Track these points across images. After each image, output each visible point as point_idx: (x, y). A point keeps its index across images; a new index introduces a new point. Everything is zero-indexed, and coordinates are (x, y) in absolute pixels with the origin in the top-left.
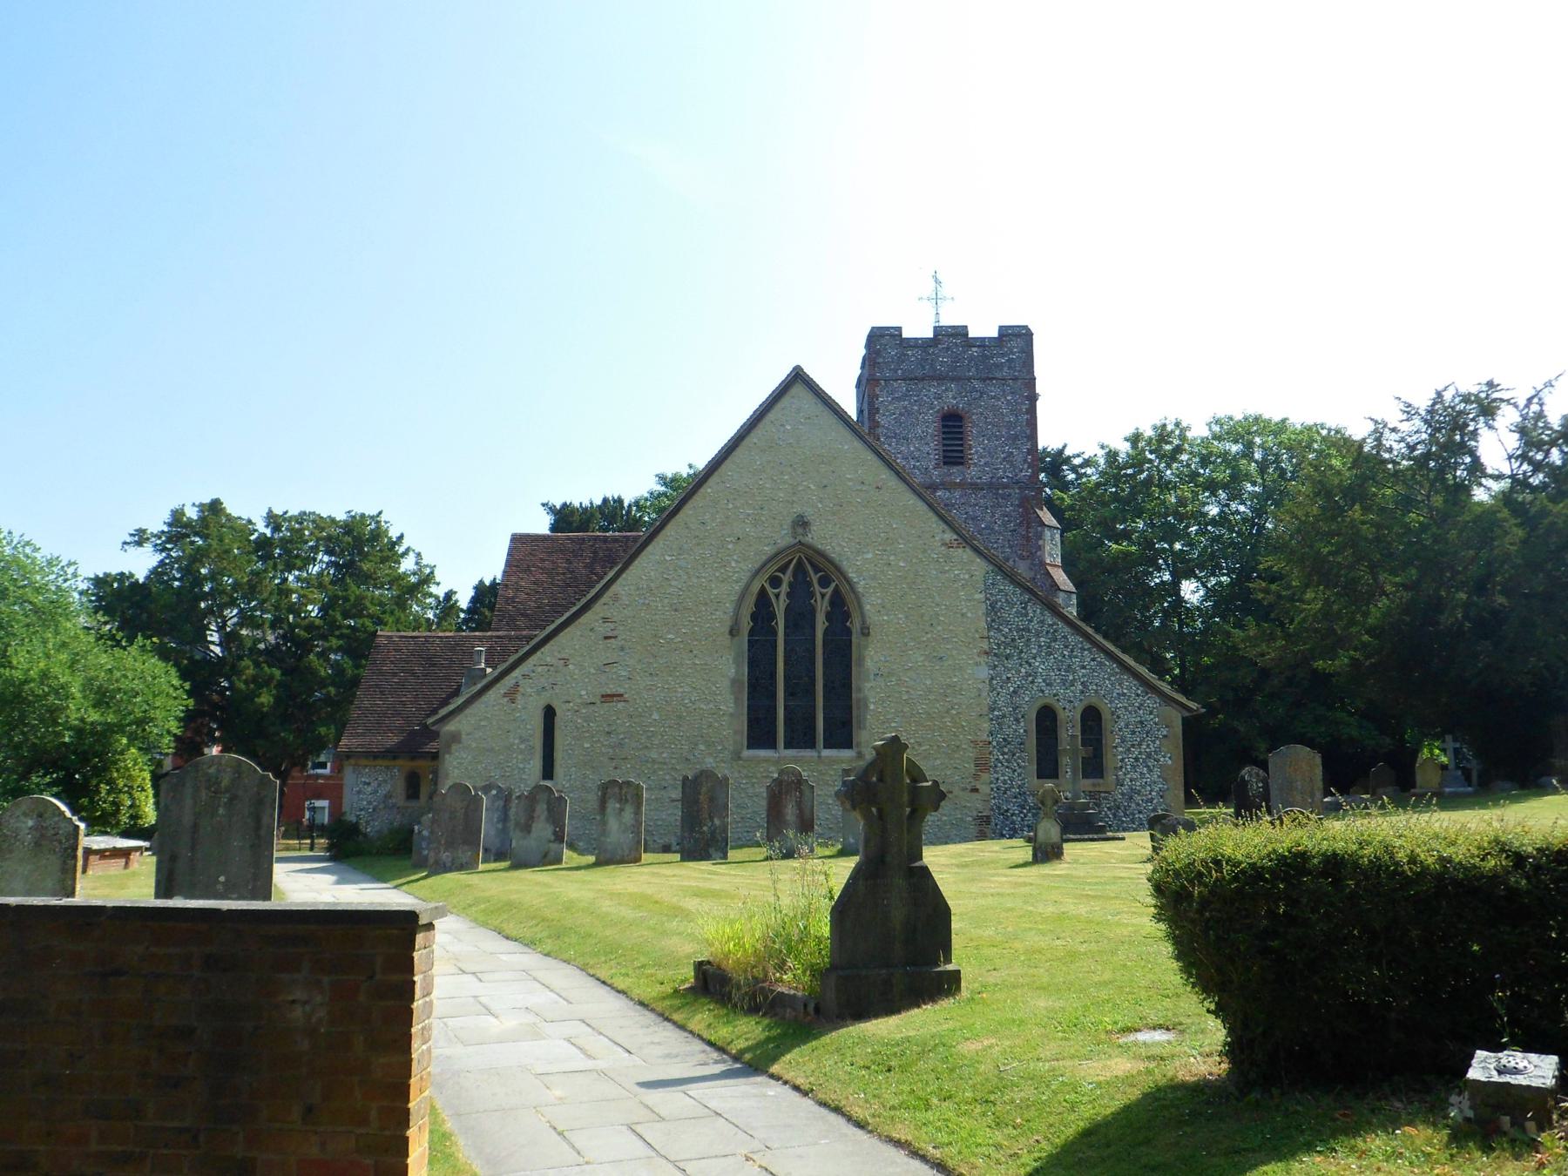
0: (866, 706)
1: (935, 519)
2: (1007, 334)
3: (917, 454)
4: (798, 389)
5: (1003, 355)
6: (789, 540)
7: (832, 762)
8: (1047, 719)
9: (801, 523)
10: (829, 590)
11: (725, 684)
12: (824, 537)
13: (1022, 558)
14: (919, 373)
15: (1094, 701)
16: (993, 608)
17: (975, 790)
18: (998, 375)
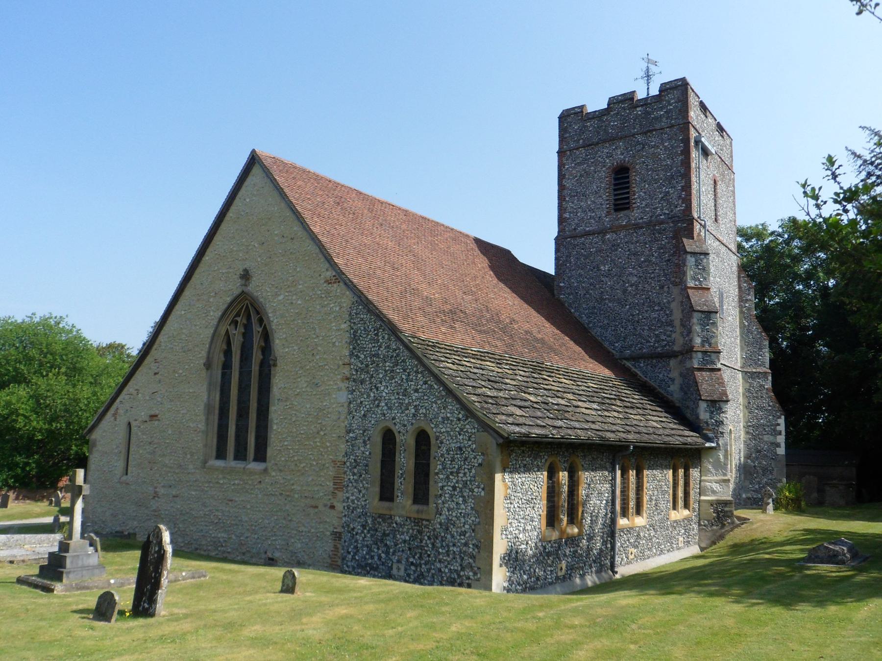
0: (272, 427)
1: (323, 259)
2: (665, 88)
3: (592, 206)
4: (256, 170)
5: (662, 109)
6: (237, 292)
7: (252, 473)
8: (389, 438)
9: (246, 276)
10: (260, 330)
11: (201, 409)
12: (261, 289)
13: (675, 284)
14: (595, 140)
15: (423, 425)
16: (355, 338)
17: (332, 507)
18: (657, 126)
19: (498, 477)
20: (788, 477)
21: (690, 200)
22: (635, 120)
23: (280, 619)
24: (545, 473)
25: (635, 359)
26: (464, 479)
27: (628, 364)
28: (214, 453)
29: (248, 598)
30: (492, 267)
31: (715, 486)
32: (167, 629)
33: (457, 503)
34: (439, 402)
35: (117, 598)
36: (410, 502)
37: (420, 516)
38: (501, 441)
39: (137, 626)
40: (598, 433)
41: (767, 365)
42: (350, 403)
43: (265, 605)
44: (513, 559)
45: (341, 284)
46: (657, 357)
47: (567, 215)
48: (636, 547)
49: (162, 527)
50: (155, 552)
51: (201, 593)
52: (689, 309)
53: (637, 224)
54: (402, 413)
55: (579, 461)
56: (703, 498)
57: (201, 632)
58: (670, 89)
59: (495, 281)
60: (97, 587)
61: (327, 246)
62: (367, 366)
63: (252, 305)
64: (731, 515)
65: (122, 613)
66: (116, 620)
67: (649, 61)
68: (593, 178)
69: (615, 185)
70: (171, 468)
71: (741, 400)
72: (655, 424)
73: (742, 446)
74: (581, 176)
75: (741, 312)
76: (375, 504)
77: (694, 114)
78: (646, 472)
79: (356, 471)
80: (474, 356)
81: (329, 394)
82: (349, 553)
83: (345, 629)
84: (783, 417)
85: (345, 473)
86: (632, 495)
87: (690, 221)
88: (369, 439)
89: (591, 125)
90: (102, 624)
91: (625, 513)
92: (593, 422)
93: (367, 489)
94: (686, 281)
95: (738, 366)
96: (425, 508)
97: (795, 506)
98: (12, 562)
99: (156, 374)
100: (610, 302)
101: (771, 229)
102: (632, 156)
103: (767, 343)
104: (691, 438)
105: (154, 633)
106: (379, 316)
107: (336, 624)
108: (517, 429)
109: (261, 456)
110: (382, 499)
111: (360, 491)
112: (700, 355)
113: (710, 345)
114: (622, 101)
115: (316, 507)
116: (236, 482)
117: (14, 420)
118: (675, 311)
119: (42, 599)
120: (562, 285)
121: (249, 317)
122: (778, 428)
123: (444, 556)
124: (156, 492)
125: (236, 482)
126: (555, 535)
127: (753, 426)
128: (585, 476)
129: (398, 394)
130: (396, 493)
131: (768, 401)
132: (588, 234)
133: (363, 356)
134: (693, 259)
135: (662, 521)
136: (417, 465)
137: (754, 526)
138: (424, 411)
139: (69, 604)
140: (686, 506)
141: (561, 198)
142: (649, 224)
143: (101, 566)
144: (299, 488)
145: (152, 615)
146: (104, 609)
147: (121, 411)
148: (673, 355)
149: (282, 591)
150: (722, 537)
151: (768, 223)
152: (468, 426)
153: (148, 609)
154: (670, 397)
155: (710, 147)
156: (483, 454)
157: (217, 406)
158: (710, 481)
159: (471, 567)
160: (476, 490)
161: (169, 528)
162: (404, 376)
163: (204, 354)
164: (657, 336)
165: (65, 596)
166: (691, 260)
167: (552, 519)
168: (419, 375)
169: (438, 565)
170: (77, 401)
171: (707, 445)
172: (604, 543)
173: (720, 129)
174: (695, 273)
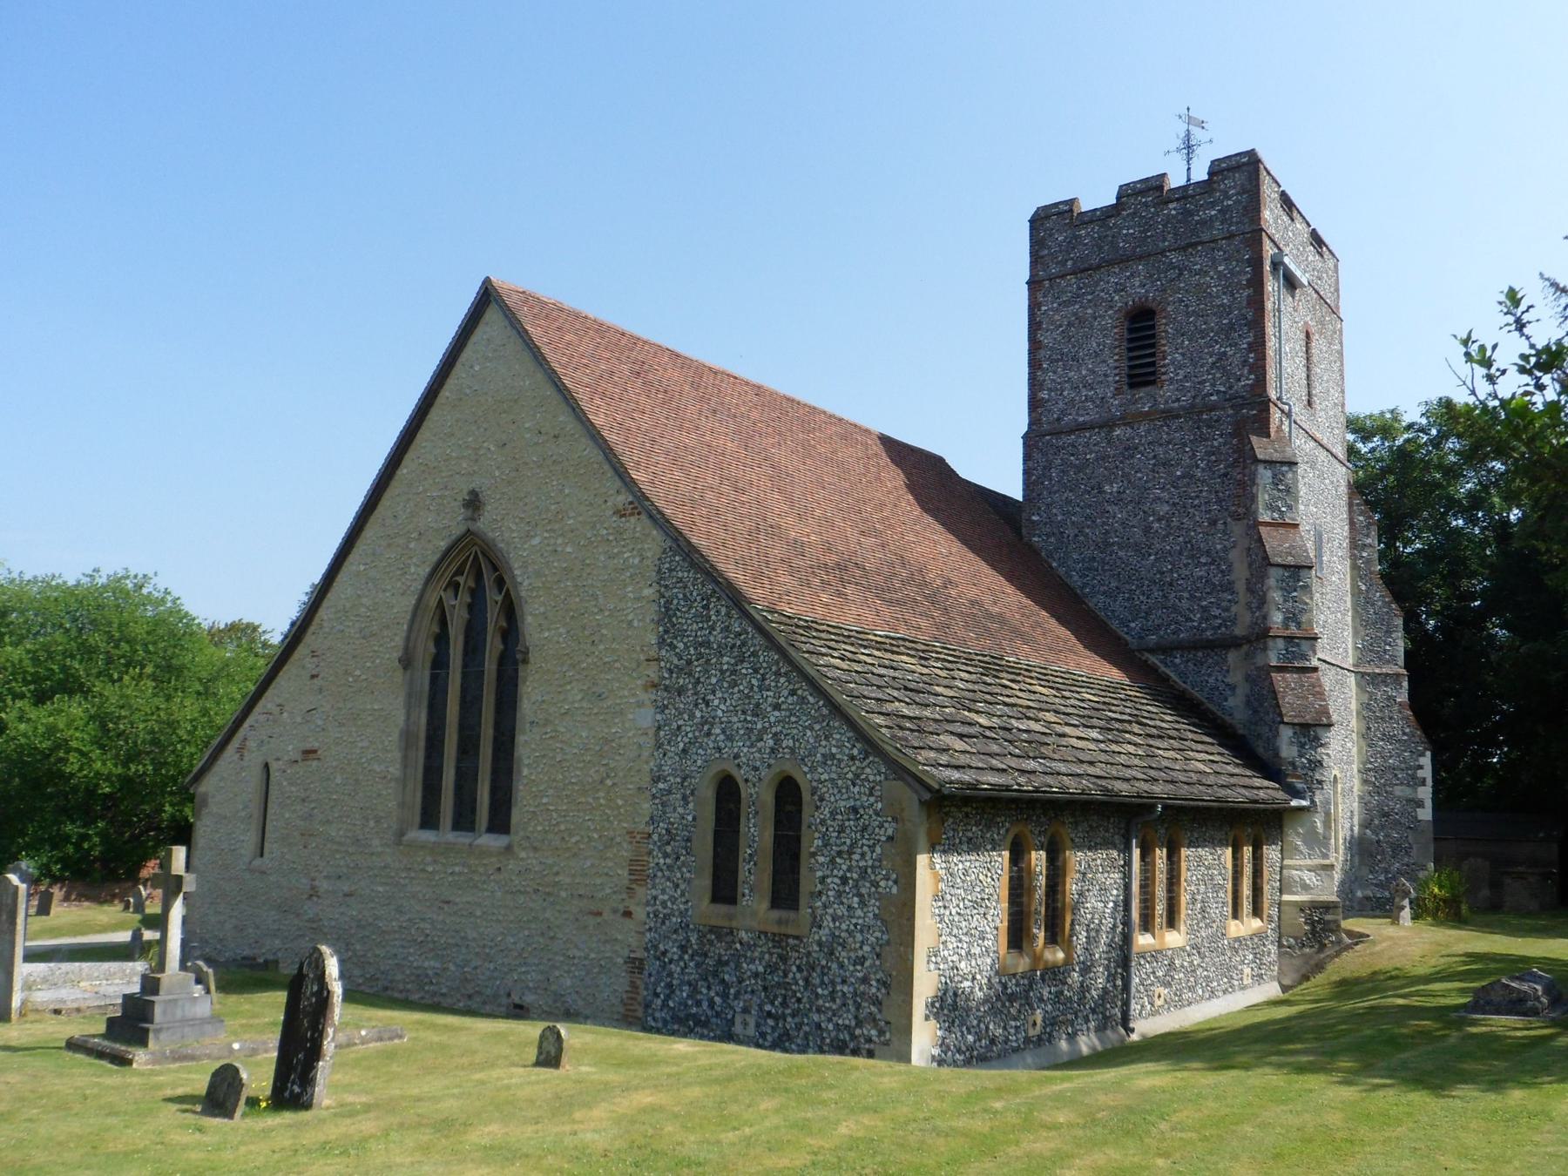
0: (520, 772)
1: (610, 473)
2: (1220, 169)
4: (492, 315)
5: (1213, 205)
6: (457, 531)
8: (727, 790)
9: (474, 503)
10: (499, 598)
12: (499, 525)
13: (1237, 518)
14: (1095, 261)
16: (667, 614)
17: (628, 914)
18: (1205, 237)
19: (922, 860)
20: (1437, 861)
21: (1264, 367)
22: (1165, 226)
23: (534, 1114)
24: (1006, 854)
25: (1165, 649)
26: (862, 864)
27: (1153, 659)
28: (417, 819)
29: (478, 1076)
30: (912, 488)
31: (1309, 877)
32: (333, 1132)
33: (850, 907)
34: (817, 727)
35: (244, 1075)
36: (765, 904)
37: (783, 930)
38: (927, 796)
39: (281, 1125)
40: (1103, 783)
41: (1401, 661)
42: (659, 728)
43: (508, 1087)
44: (949, 1006)
45: (644, 517)
46: (1205, 648)
47: (1044, 395)
48: (1167, 985)
49: (325, 949)
50: (313, 994)
51: (394, 1068)
52: (1261, 562)
53: (1169, 411)
54: (752, 746)
55: (1066, 832)
56: (1286, 897)
57: (394, 1136)
58: (1228, 169)
59: (917, 511)
60: (209, 1056)
61: (619, 449)
62: (689, 662)
63: (484, 554)
64: (1336, 929)
65: (253, 1102)
66: (244, 1115)
67: (1190, 120)
68: (1091, 328)
69: (1130, 340)
70: (340, 843)
71: (1354, 722)
72: (1201, 766)
73: (1356, 804)
74: (1070, 324)
75: (1354, 567)
76: (703, 909)
77: (1270, 214)
78: (1184, 852)
79: (669, 849)
80: (879, 646)
81: (622, 713)
82: (657, 995)
83: (650, 1131)
84: (1428, 753)
85: (650, 853)
86: (1160, 891)
87: (1264, 405)
88: (692, 793)
89: (1088, 234)
90: (217, 1121)
91: (1147, 925)
92: (1091, 763)
93: (688, 881)
94: (1256, 512)
95: (1349, 662)
96: (792, 915)
97: (1451, 912)
98: (57, 1012)
99: (313, 677)
100: (1121, 548)
101: (1407, 419)
102: (1161, 289)
103: (1399, 622)
104: (1265, 790)
105: (310, 1138)
106: (711, 574)
107: (633, 1122)
108: (956, 775)
109: (500, 822)
110: (715, 899)
111: (677, 886)
112: (1280, 643)
113: (1299, 625)
114: (1142, 192)
115: (599, 914)
116: (457, 869)
117: (61, 760)
118: (1237, 565)
119: (108, 1077)
120: (1035, 518)
121: (479, 576)
122: (1420, 773)
123: (828, 1002)
124: (313, 888)
125: (457, 869)
126: (1023, 964)
127: (1375, 770)
128: (1077, 859)
129: (744, 712)
130: (740, 890)
131: (1402, 724)
132: (1082, 427)
133: (681, 645)
134: (1269, 473)
135: (1213, 939)
136: (778, 839)
137: (1378, 948)
138: (791, 743)
139: (160, 1086)
140: (1257, 911)
141: (1034, 364)
142: (1192, 411)
143: (216, 1019)
144: (568, 880)
145: (307, 1106)
146: (222, 1095)
147: (252, 744)
148: (1234, 643)
149: (538, 1064)
150: (1319, 967)
151: (1401, 409)
152: (868, 770)
153: (299, 1096)
154: (1227, 718)
155: (1298, 273)
156: (895, 819)
157: (423, 735)
158: (1299, 868)
159: (874, 1020)
160: (882, 884)
161: (337, 952)
162: (754, 682)
163: (399, 641)
164: (1205, 609)
165: (152, 1073)
166: (1264, 475)
167: (1017, 936)
168: (782, 680)
169: (816, 1017)
170: (173, 725)
171: (1294, 803)
172: (1111, 978)
173: (1317, 241)
174: (1273, 498)
